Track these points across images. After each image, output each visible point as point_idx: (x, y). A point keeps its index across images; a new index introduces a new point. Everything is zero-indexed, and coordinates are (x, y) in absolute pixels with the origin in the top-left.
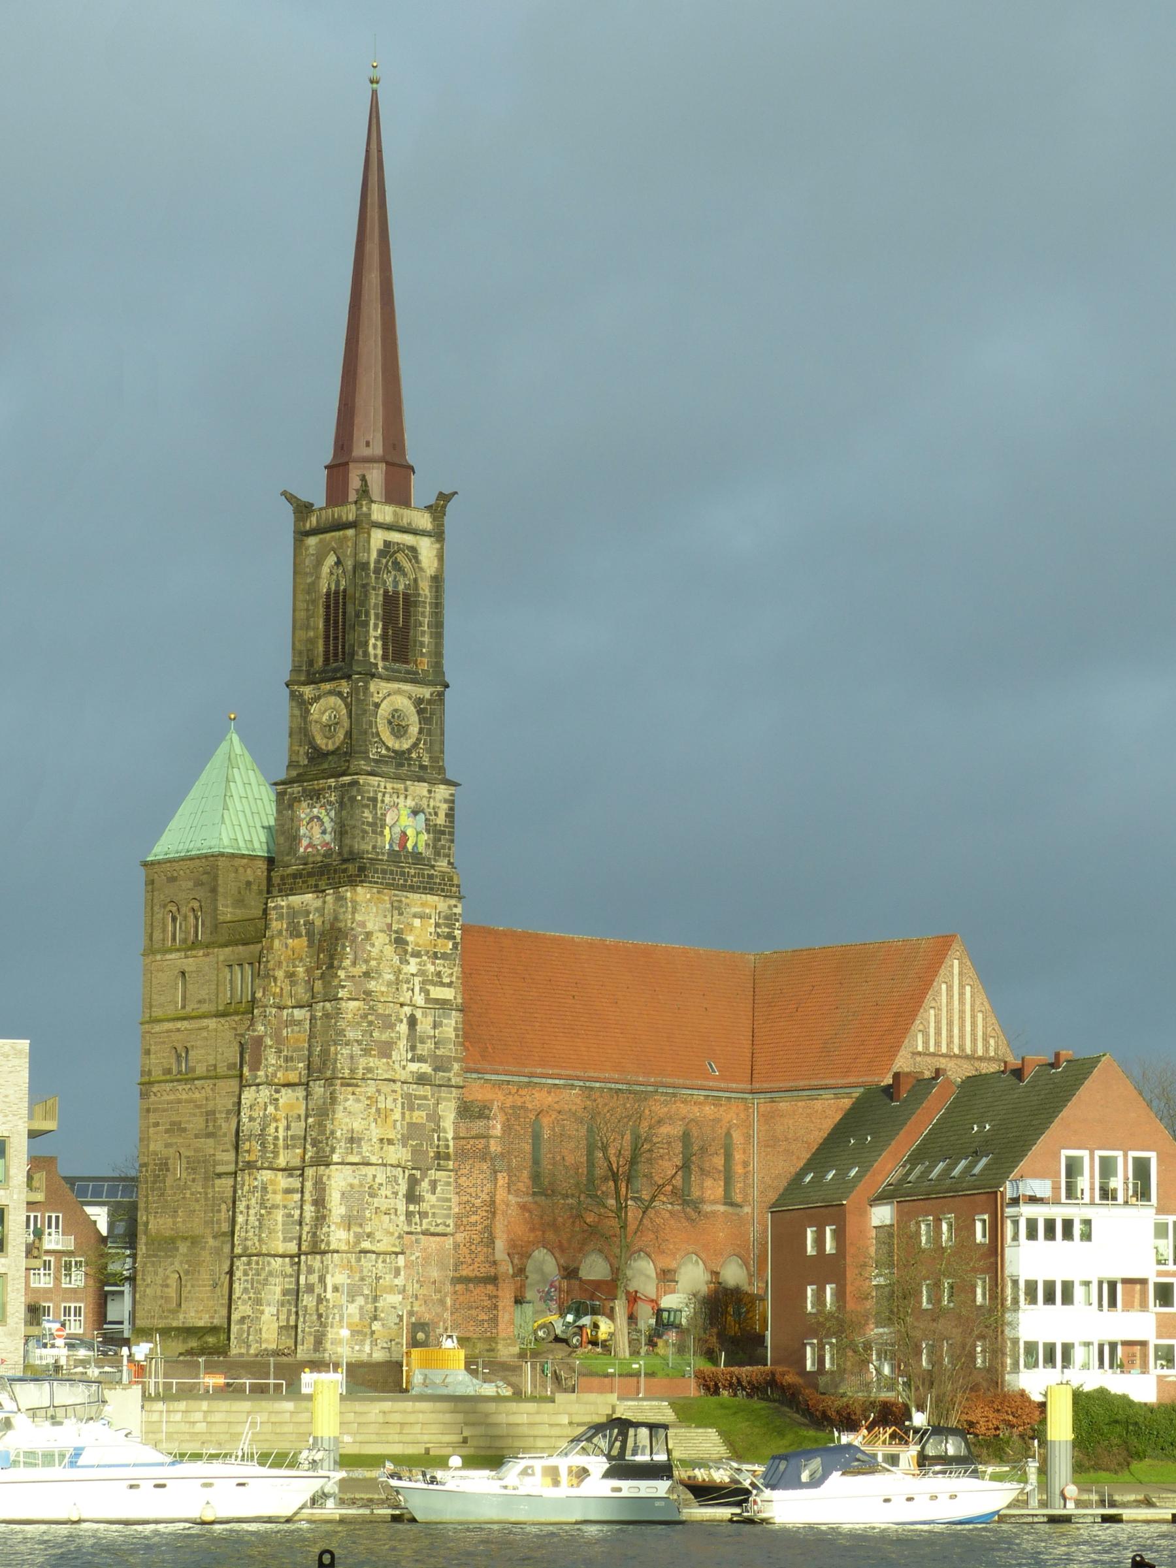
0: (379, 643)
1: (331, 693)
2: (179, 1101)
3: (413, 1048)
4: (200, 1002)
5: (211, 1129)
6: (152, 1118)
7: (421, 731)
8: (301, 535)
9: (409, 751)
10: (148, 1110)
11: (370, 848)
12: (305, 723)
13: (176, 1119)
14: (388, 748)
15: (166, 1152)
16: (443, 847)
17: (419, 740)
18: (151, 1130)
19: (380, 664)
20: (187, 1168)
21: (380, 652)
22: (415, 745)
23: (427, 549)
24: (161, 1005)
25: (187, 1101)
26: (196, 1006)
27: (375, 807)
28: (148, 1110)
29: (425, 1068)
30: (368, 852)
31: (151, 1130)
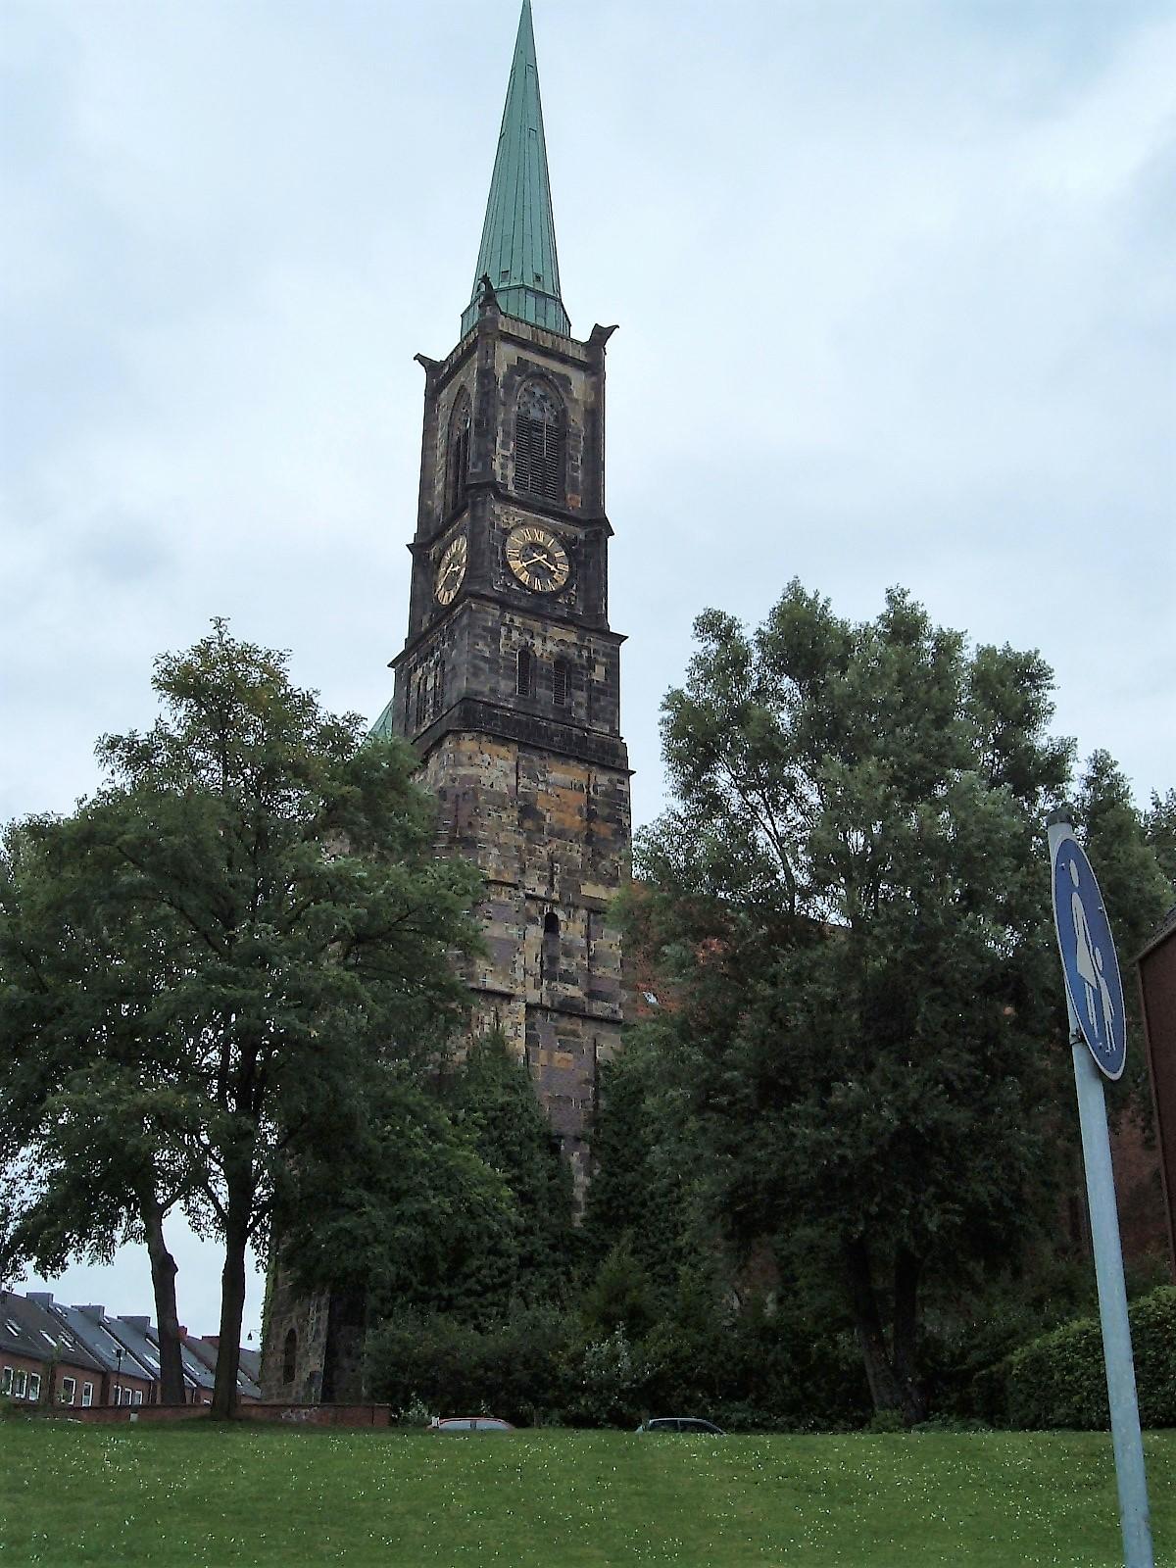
0: (511, 465)
1: (454, 537)
3: (553, 960)
7: (572, 575)
9: (555, 595)
11: (486, 689)
14: (521, 584)
16: (603, 709)
17: (568, 585)
19: (511, 487)
21: (511, 473)
22: (564, 590)
23: (578, 381)
27: (496, 640)
29: (573, 991)
30: (481, 693)
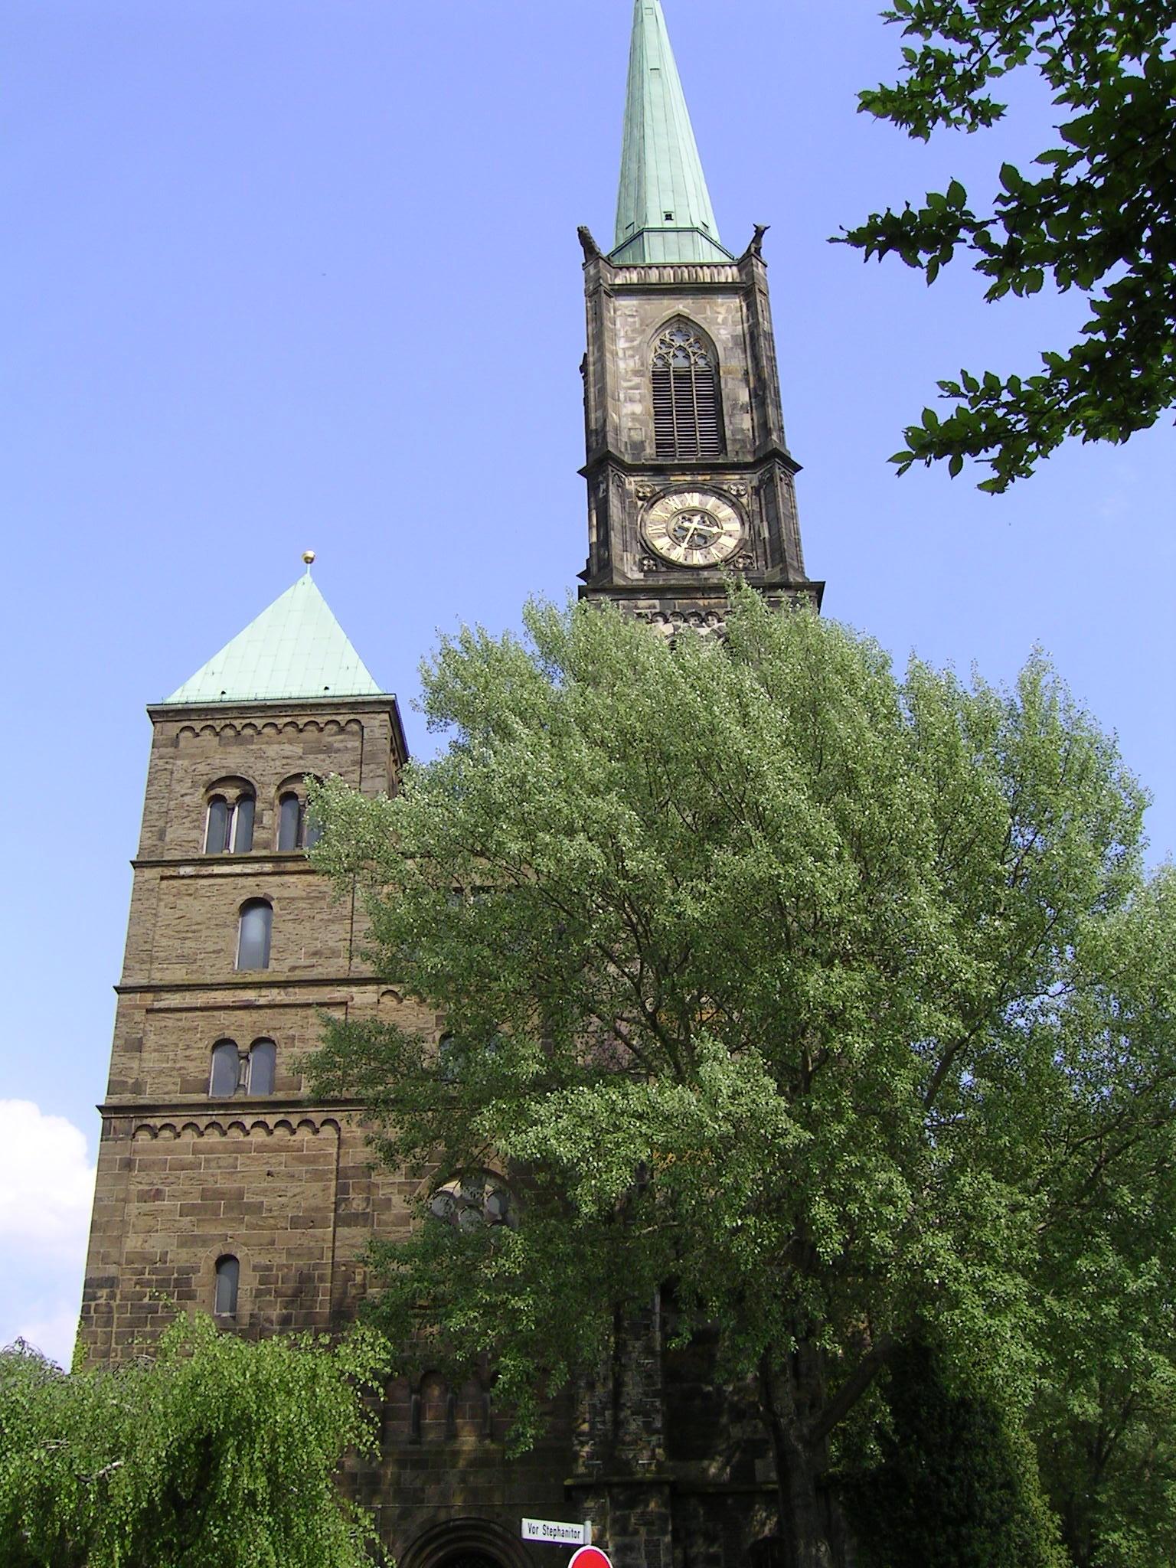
1: (693, 488)
2: (239, 1149)
4: (315, 954)
5: (357, 1203)
6: (140, 1181)
8: (597, 294)
10: (128, 1165)
12: (633, 522)
13: (223, 1184)
15: (180, 1257)
18: (134, 1207)
20: (259, 1294)
24: (182, 958)
25: (278, 1149)
26: (303, 962)
28: (128, 1165)
31: (134, 1207)
